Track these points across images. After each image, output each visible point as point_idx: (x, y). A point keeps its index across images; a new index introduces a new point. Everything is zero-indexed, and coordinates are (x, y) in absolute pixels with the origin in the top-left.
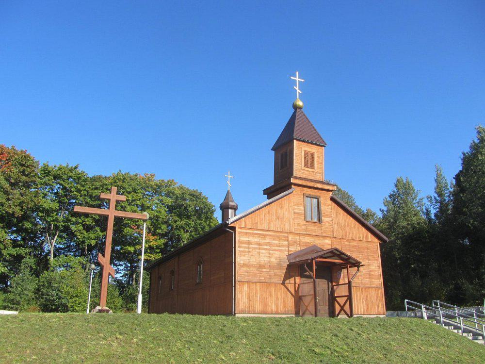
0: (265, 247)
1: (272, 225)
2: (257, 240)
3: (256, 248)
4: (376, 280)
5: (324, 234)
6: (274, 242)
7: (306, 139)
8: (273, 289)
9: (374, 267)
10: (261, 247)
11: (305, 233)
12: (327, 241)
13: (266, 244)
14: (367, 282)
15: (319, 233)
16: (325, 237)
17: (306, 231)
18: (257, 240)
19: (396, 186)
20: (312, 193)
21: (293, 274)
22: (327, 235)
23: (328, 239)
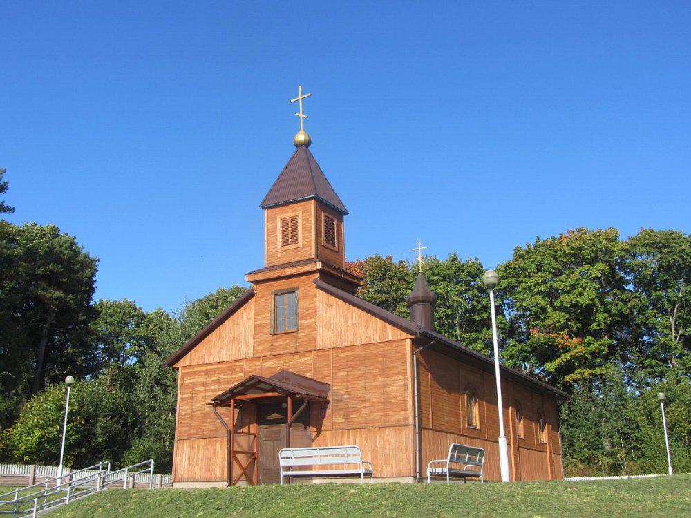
0: (213, 387)
1: (223, 354)
2: (202, 379)
3: (201, 391)
4: (340, 421)
5: (301, 349)
6: (225, 377)
7: (280, 201)
8: (219, 446)
9: (394, 388)
10: (207, 388)
11: (269, 354)
12: (306, 359)
13: (214, 382)
14: (378, 418)
15: (292, 347)
16: (302, 353)
17: (270, 350)
18: (202, 379)
19: (400, 263)
20: (286, 287)
21: (247, 421)
22: (306, 349)
23: (307, 355)
